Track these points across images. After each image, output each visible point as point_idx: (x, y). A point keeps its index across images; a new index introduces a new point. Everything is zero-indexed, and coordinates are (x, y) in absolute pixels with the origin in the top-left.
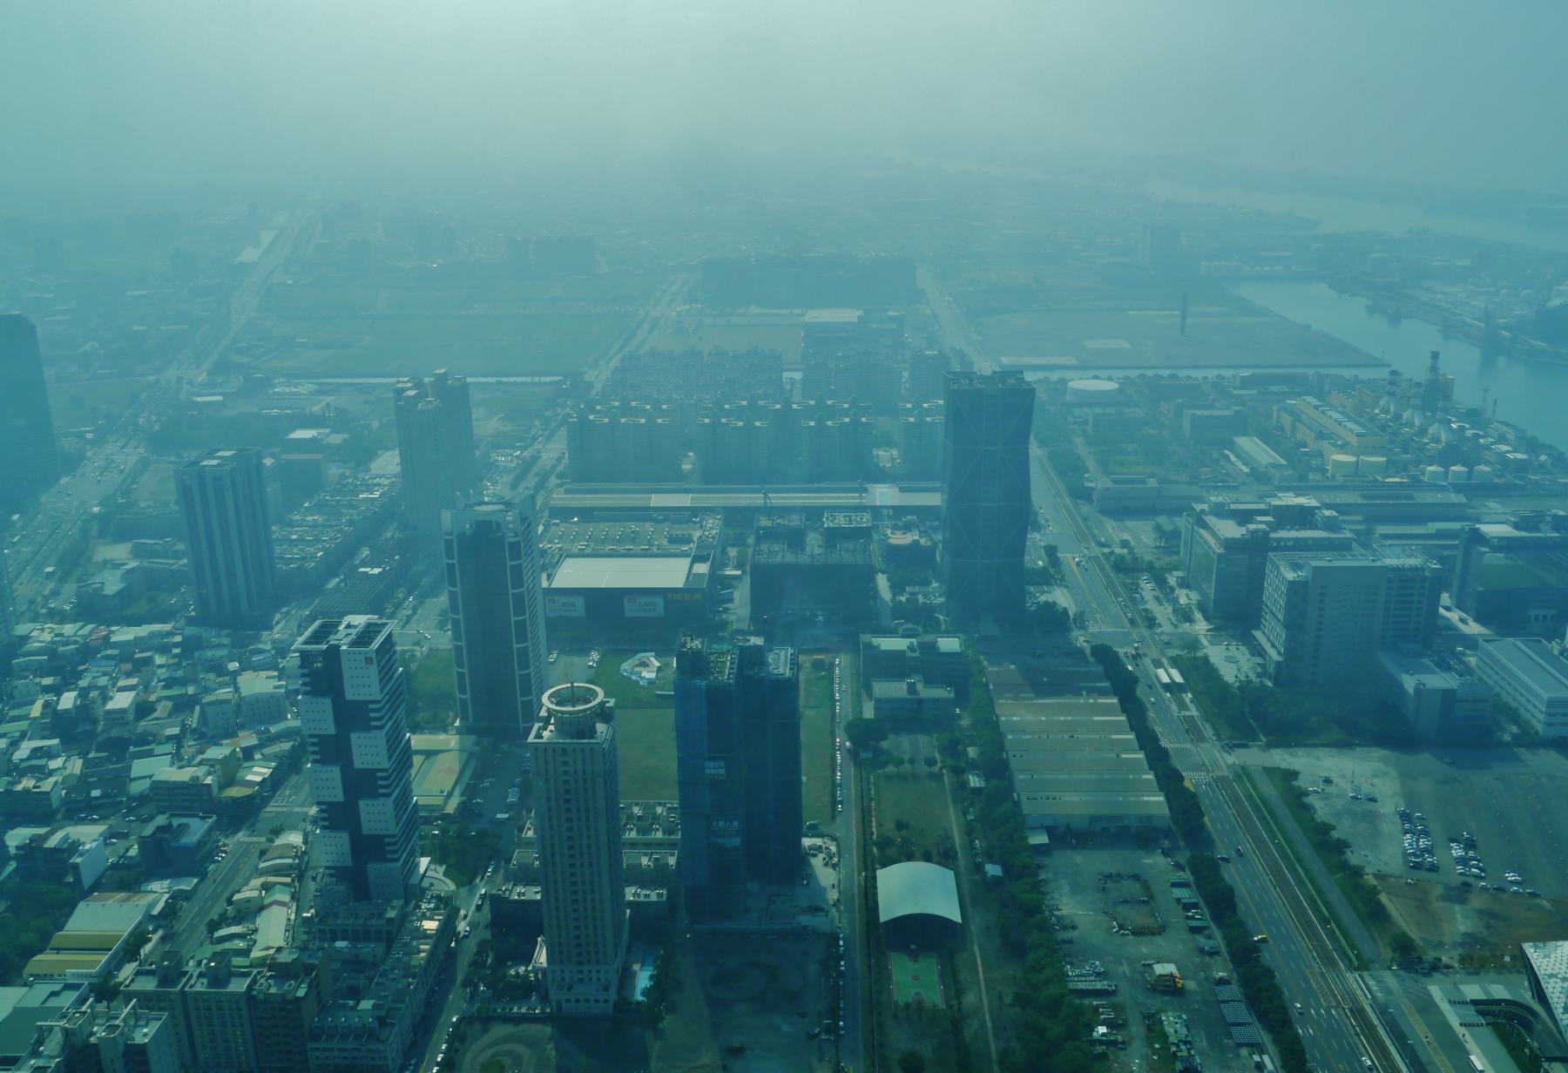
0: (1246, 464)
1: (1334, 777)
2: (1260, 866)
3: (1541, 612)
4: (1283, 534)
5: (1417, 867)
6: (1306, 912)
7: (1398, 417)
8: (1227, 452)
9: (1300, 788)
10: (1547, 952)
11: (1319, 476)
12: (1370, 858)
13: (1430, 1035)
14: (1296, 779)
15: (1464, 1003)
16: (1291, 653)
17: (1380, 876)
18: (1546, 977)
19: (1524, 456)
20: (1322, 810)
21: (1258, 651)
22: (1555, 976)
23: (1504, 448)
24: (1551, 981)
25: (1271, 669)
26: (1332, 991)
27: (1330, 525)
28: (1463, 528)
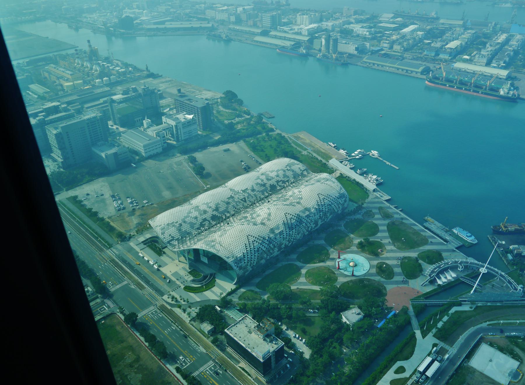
0: (36, 94)
1: (89, 192)
2: (73, 230)
4: (51, 117)
5: (119, 210)
6: (91, 238)
7: (83, 65)
8: (28, 92)
9: (79, 200)
10: (154, 220)
11: (62, 92)
12: (105, 213)
13: (133, 257)
14: (77, 198)
16: (65, 158)
17: (109, 218)
19: (124, 70)
20: (88, 204)
21: (55, 160)
22: (157, 226)
23: (118, 68)
25: (61, 165)
26: (104, 258)
27: (65, 110)
28: (108, 99)
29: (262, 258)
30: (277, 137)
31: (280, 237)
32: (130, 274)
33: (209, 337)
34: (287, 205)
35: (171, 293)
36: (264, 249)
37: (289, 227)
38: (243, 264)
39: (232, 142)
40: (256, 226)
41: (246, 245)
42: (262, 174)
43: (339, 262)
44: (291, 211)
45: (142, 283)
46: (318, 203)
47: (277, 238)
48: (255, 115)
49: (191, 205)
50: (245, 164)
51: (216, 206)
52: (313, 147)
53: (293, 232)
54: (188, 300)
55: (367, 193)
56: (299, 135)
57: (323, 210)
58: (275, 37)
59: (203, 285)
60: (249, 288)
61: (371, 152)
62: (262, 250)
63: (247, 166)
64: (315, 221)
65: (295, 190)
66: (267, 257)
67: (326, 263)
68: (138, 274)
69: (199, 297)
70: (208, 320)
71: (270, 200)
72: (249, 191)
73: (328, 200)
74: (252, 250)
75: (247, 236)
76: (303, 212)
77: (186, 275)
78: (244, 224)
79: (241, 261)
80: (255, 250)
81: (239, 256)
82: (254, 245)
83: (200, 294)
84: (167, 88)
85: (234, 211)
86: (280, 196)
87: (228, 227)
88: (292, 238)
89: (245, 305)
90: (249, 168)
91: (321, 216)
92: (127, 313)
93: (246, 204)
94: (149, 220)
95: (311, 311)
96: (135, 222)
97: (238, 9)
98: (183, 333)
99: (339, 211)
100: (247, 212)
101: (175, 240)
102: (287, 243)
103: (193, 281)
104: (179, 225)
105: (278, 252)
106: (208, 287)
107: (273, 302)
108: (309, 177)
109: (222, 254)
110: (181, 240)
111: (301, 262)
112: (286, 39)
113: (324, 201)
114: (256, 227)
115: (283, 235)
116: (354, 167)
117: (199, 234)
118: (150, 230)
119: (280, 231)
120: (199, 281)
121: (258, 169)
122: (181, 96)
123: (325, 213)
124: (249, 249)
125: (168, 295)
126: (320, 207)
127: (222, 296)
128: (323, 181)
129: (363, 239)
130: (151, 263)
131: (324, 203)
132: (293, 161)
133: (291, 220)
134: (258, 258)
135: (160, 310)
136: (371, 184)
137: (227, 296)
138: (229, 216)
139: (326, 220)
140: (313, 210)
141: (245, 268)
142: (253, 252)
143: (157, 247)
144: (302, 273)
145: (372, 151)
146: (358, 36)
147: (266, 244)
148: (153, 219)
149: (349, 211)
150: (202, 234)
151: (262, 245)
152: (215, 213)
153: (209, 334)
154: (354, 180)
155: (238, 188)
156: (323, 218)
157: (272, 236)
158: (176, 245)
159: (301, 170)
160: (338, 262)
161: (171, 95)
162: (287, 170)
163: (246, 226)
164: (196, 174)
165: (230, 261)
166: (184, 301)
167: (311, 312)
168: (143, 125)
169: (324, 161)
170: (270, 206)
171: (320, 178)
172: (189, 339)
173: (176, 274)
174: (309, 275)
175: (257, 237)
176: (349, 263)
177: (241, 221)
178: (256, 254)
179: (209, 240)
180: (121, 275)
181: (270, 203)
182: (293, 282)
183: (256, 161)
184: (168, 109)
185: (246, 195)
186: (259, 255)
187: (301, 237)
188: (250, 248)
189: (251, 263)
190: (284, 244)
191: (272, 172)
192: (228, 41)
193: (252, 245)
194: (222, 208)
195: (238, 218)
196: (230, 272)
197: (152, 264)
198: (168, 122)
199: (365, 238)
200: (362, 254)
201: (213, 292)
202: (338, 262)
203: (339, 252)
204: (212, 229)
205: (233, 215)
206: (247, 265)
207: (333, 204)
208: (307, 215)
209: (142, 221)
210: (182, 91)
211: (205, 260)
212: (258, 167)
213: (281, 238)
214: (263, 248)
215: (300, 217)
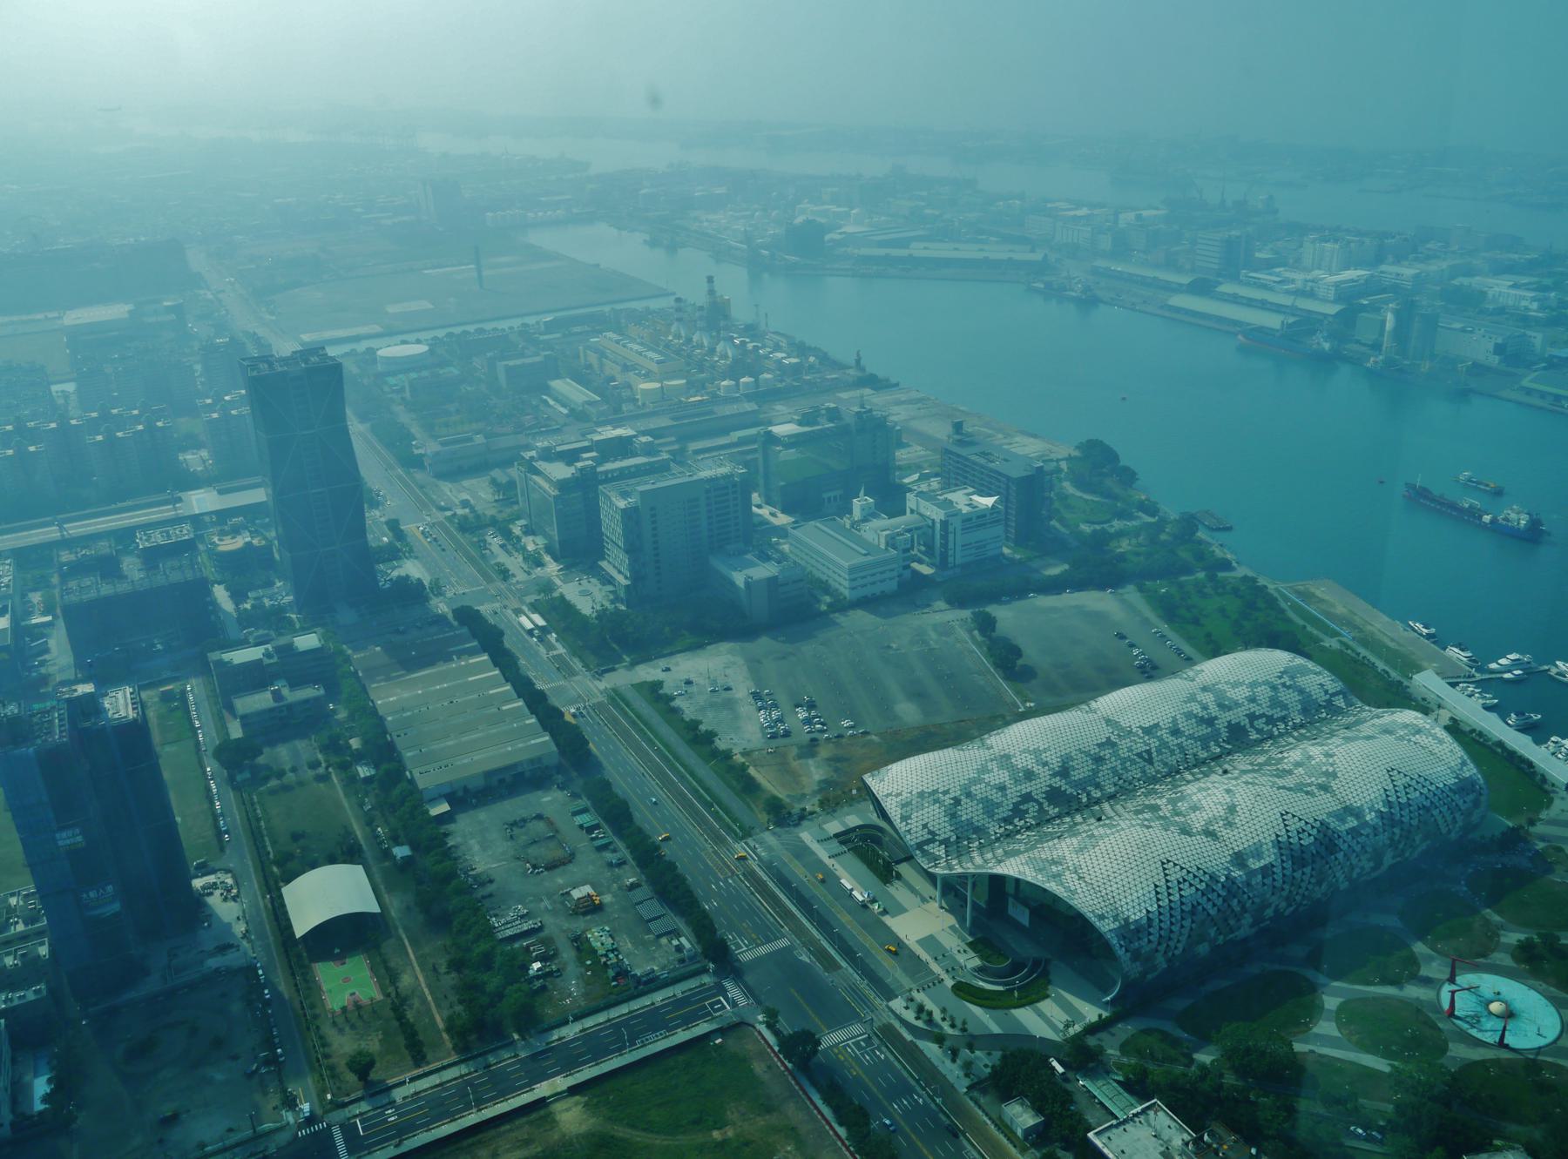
0: (564, 406)
1: (693, 677)
3: (832, 494)
4: (609, 466)
5: (774, 736)
6: (693, 804)
7: (689, 340)
8: (545, 397)
9: (666, 695)
11: (631, 407)
12: (735, 741)
13: (808, 875)
14: (661, 688)
16: (637, 577)
17: (745, 754)
20: (688, 709)
21: (607, 580)
22: (890, 794)
23: (780, 355)
25: (622, 594)
26: (725, 863)
27: (649, 450)
28: (759, 433)
30: (1243, 588)
31: (1264, 884)
33: (1028, 1149)
34: (1290, 789)
35: (915, 994)
36: (1213, 912)
37: (1292, 856)
38: (1143, 945)
39: (1102, 587)
40: (1191, 836)
41: (1158, 889)
42: (1205, 689)
43: (1457, 994)
44: (1310, 805)
45: (832, 952)
46: (1387, 796)
47: (1253, 883)
48: (1173, 516)
49: (988, 749)
51: (1064, 763)
52: (1355, 627)
53: (1303, 873)
54: (964, 1023)
56: (1312, 590)
57: (1402, 822)
58: (1235, 299)
59: (1014, 989)
60: (1153, 1024)
61: (1557, 666)
63: (1149, 660)
65: (1311, 748)
67: (1401, 988)
68: (824, 924)
69: (998, 1023)
70: (1026, 1097)
71: (1226, 766)
72: (1164, 734)
75: (1163, 863)
77: (959, 951)
78: (1151, 827)
79: (1140, 935)
80: (1184, 907)
81: (1133, 917)
82: (1182, 893)
83: (999, 1013)
84: (913, 418)
85: (1115, 785)
86: (1261, 759)
88: (1300, 891)
89: (1145, 1073)
90: (1155, 668)
91: (1396, 838)
92: (787, 1029)
95: (1360, 1131)
97: (1122, 216)
98: (948, 1122)
100: (1156, 793)
102: (1284, 904)
103: (980, 970)
105: (1252, 926)
109: (1084, 902)
112: (1268, 306)
113: (1407, 793)
114: (1189, 839)
115: (1274, 880)
117: (1008, 836)
119: (1263, 863)
120: (997, 975)
122: (961, 443)
123: (1409, 832)
126: (1392, 810)
127: (1072, 1031)
129: (1537, 934)
131: (1408, 799)
132: (1300, 660)
133: (1301, 836)
134: (1189, 936)
135: (881, 1040)
139: (1407, 854)
140: (1370, 817)
142: (1177, 913)
145: (1558, 663)
146: (1501, 311)
147: (1219, 895)
148: (876, 772)
150: (1018, 837)
151: (1205, 898)
152: (1058, 782)
153: (1026, 1138)
154: (1500, 744)
156: (1401, 846)
157: (1237, 873)
158: (941, 858)
159: (1326, 692)
160: (1453, 993)
161: (925, 440)
162: (1284, 685)
163: (1156, 831)
165: (1106, 927)
166: (953, 1026)
167: (1358, 1136)
168: (850, 512)
169: (1394, 675)
171: (1394, 722)
172: (965, 1142)
173: (929, 942)
174: (1348, 1015)
178: (1187, 923)
179: (1044, 856)
180: (772, 920)
181: (1229, 775)
183: (1178, 649)
184: (916, 476)
185: (1154, 743)
188: (1170, 901)
189: (1168, 945)
190: (1273, 905)
191: (1235, 685)
192: (1088, 302)
193: (1174, 891)
195: (1129, 805)
198: (922, 510)
199: (1543, 931)
200: (1531, 982)
201: (1040, 1014)
202: (1453, 993)
203: (1454, 961)
205: (1112, 797)
206: (1157, 951)
207: (1436, 807)
210: (967, 428)
211: (1023, 916)
214: (1209, 906)
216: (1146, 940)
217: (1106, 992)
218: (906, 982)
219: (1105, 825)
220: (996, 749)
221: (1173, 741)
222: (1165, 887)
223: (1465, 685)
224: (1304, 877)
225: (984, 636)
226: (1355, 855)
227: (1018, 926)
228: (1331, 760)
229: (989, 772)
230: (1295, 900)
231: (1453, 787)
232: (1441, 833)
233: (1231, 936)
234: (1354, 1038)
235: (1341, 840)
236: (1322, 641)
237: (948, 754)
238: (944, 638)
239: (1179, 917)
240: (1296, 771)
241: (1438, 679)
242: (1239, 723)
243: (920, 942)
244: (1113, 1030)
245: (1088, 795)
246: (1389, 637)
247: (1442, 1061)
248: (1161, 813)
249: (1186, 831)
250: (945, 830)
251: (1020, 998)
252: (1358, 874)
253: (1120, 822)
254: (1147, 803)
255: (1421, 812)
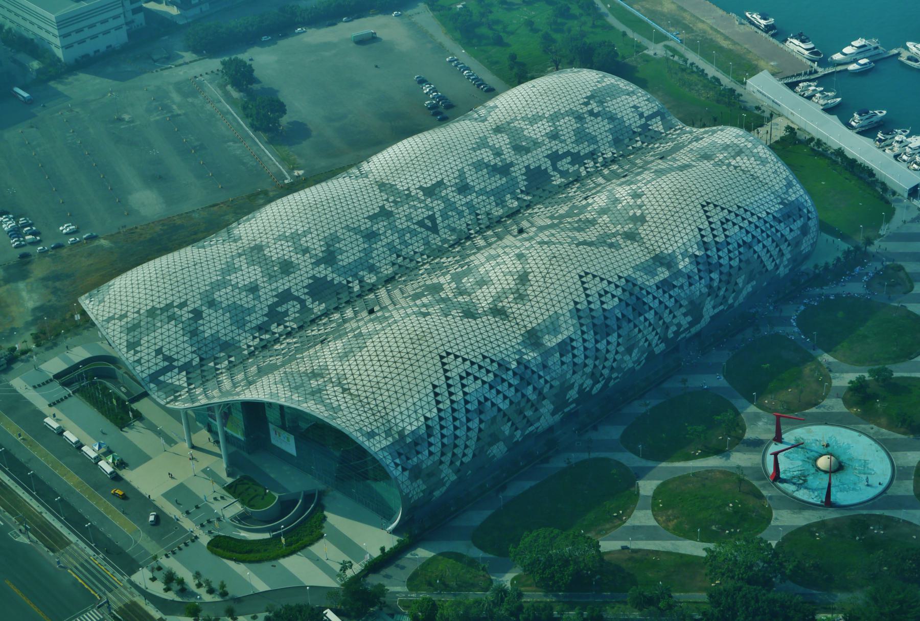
10: (101, 297)
13: (23, 432)
15: (48, 382)
18: (104, 323)
24: (110, 325)
29: (495, 438)
31: (563, 363)
32: (12, 492)
34: (590, 244)
35: (164, 562)
36: (504, 406)
37: (594, 325)
38: (424, 459)
39: (385, 10)
41: (437, 390)
42: (498, 130)
43: (780, 456)
45: (57, 525)
46: (702, 236)
47: (550, 363)
49: (235, 241)
50: (434, 90)
51: (328, 246)
52: (687, 28)
53: (608, 343)
55: (888, 202)
57: (721, 265)
59: (279, 536)
60: (446, 547)
61: (907, 48)
62: (495, 409)
63: (441, 98)
64: (692, 302)
65: (619, 189)
66: (512, 436)
67: (728, 457)
71: (525, 224)
72: (449, 193)
73: (741, 228)
74: (460, 406)
75: (442, 357)
76: (648, 269)
77: (215, 499)
78: (429, 314)
79: (419, 448)
80: (469, 406)
81: (409, 428)
82: (466, 389)
83: (266, 566)
85: (394, 264)
86: (563, 209)
87: (370, 325)
90: (450, 106)
91: (715, 284)
93: (435, 241)
94: (83, 297)
96: (30, 305)
99: (781, 269)
100: (441, 268)
101: (176, 370)
102: (589, 382)
103: (243, 519)
104: (191, 315)
105: (553, 414)
106: (297, 541)
107: (533, 596)
108: (673, 140)
110: (199, 371)
111: (639, 456)
113: (725, 230)
114: (473, 322)
115: (574, 356)
116: (840, 104)
118: (86, 333)
119: (560, 338)
120: (267, 519)
121: (482, 111)
123: (730, 275)
124: (446, 405)
125: (152, 571)
126: (709, 253)
127: (349, 573)
128: (721, 157)
129: (870, 372)
130: (90, 451)
131: (726, 236)
132: (611, 80)
133: (603, 299)
134: (479, 439)
136: (903, 166)
137: (366, 576)
138: (374, 285)
139: (730, 301)
140: (683, 264)
141: (431, 475)
142: (461, 415)
143: (110, 396)
144: (642, 492)
147: (510, 385)
148: (95, 292)
149: (816, 266)
150: (277, 347)
151: (494, 391)
152: (322, 271)
154: (840, 152)
155: (408, 182)
156: (721, 293)
157: (531, 356)
158: (179, 388)
159: (641, 115)
160: (776, 454)
162: (591, 113)
163: (435, 318)
164: (252, 126)
165: (376, 446)
166: (211, 591)
169: (727, 81)
170: (527, 249)
171: (714, 144)
173: (180, 494)
175: (479, 360)
176: (816, 460)
177: (418, 302)
178: (474, 424)
179: (302, 369)
181: (525, 235)
182: (607, 526)
183: (477, 79)
185: (438, 206)
186: (482, 426)
187: (638, 362)
188: (452, 402)
189: (454, 454)
191: (534, 120)
194: (349, 255)
195: (409, 290)
196: (380, 487)
197: (93, 455)
201: (316, 560)
202: (776, 454)
203: (778, 417)
204: (313, 331)
205: (390, 280)
206: (441, 462)
207: (759, 241)
208: (661, 282)
209: (54, 299)
211: (287, 444)
212: (482, 102)
213: (565, 367)
214: (499, 400)
215: (637, 288)
216: (426, 452)
217: (389, 518)
218: (150, 546)
219: (378, 317)
220: (245, 241)
221: (460, 200)
222: (445, 386)
223: (805, 84)
224: (609, 347)
225: (240, 91)
226: (667, 311)
227: (282, 455)
228: (639, 202)
229: (236, 270)
230: (602, 375)
231: (777, 215)
232: (767, 270)
233: (531, 429)
234: (672, 524)
235: (650, 296)
236: (646, 48)
237: (188, 254)
238: (190, 100)
239: (464, 420)
240: (600, 220)
241: (774, 81)
242: (540, 166)
243: (167, 495)
244: (401, 562)
245: (361, 281)
246: (722, 34)
247: (764, 535)
248: (443, 296)
249: (469, 313)
250: (185, 353)
251: (289, 544)
252: (674, 333)
253: (394, 313)
254: (428, 282)
255: (741, 250)
